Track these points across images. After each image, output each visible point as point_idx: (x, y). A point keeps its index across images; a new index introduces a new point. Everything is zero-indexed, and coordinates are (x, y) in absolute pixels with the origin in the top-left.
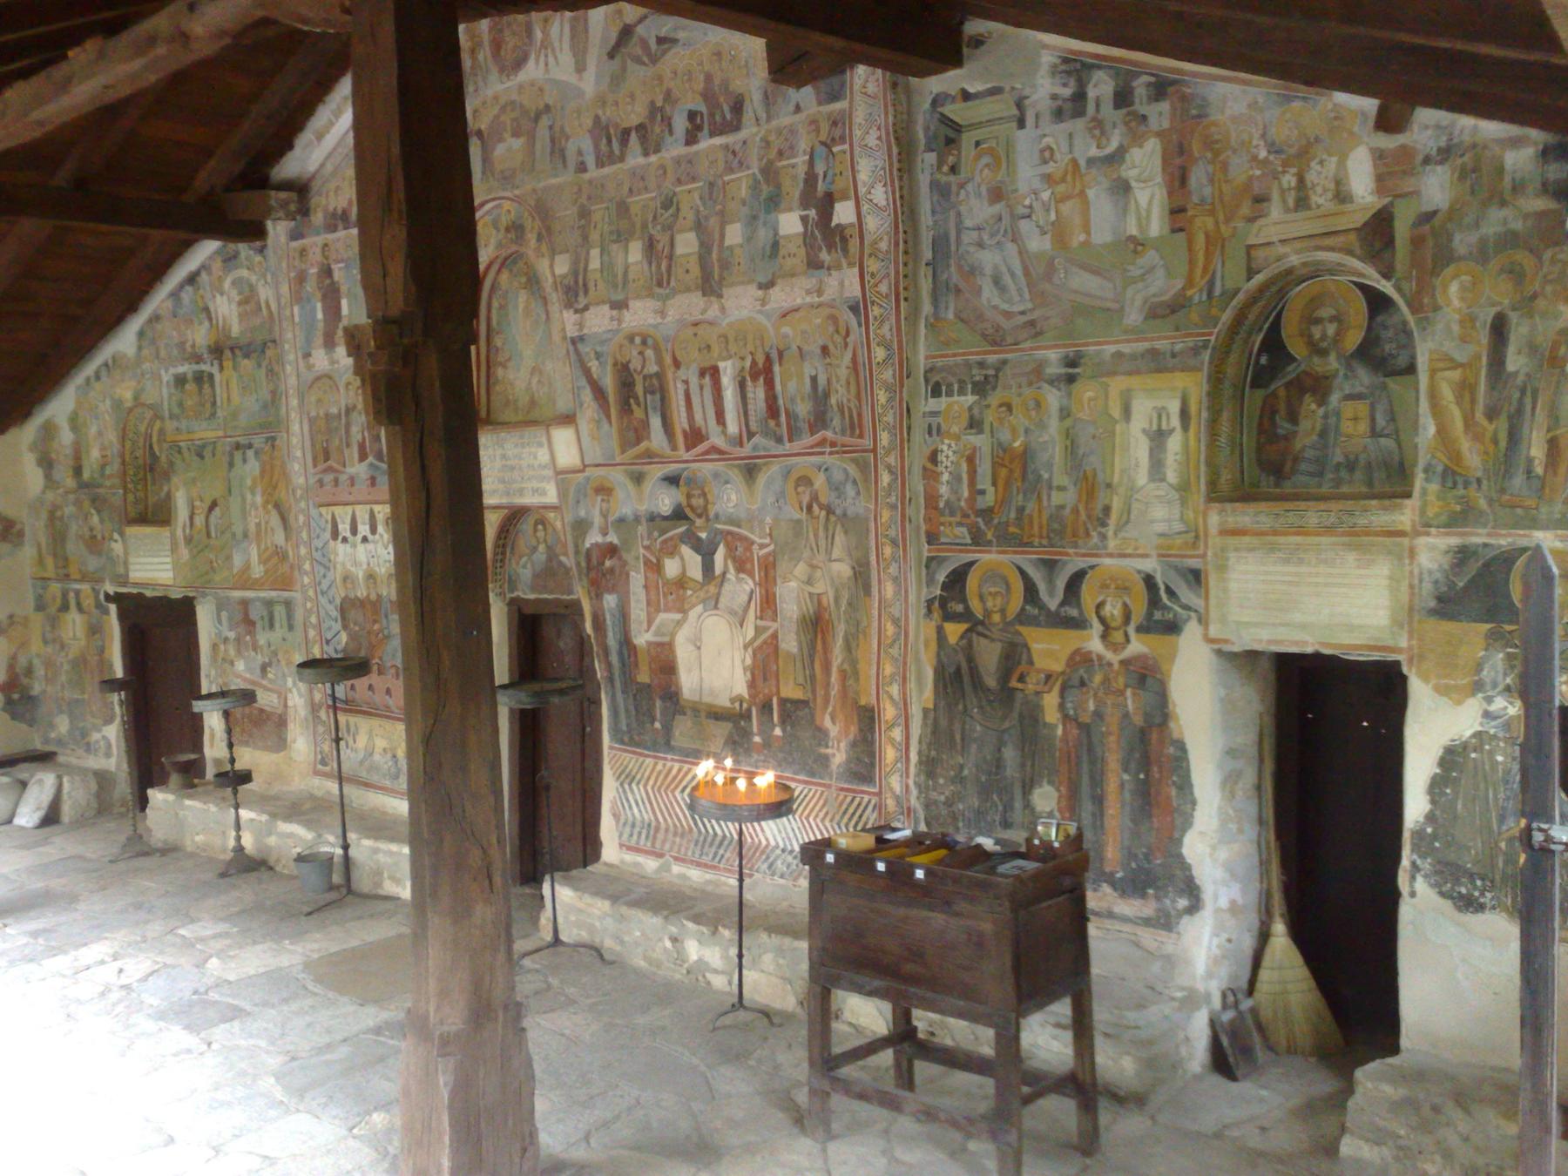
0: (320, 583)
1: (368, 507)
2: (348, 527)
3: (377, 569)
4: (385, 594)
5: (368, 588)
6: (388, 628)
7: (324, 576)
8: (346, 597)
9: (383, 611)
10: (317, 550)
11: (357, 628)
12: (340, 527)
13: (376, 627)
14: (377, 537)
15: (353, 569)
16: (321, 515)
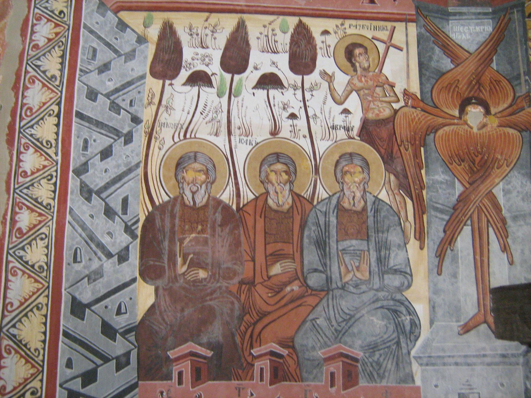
0: (79, 172)
1: (292, 21)
2: (217, 55)
3: (305, 144)
4: (322, 193)
5: (265, 181)
6: (324, 268)
7: (106, 154)
8: (178, 199)
9: (311, 232)
10: (92, 95)
11: (202, 274)
12: (188, 54)
13: (276, 269)
14: (311, 79)
15: (221, 141)
16: (123, 26)
